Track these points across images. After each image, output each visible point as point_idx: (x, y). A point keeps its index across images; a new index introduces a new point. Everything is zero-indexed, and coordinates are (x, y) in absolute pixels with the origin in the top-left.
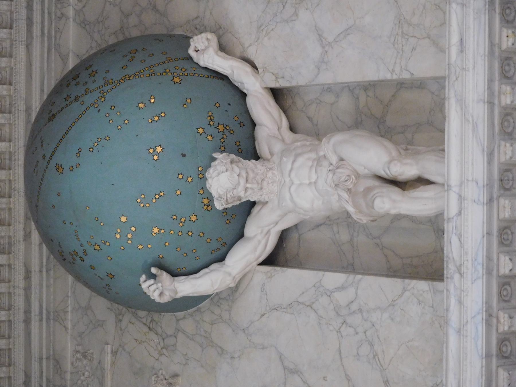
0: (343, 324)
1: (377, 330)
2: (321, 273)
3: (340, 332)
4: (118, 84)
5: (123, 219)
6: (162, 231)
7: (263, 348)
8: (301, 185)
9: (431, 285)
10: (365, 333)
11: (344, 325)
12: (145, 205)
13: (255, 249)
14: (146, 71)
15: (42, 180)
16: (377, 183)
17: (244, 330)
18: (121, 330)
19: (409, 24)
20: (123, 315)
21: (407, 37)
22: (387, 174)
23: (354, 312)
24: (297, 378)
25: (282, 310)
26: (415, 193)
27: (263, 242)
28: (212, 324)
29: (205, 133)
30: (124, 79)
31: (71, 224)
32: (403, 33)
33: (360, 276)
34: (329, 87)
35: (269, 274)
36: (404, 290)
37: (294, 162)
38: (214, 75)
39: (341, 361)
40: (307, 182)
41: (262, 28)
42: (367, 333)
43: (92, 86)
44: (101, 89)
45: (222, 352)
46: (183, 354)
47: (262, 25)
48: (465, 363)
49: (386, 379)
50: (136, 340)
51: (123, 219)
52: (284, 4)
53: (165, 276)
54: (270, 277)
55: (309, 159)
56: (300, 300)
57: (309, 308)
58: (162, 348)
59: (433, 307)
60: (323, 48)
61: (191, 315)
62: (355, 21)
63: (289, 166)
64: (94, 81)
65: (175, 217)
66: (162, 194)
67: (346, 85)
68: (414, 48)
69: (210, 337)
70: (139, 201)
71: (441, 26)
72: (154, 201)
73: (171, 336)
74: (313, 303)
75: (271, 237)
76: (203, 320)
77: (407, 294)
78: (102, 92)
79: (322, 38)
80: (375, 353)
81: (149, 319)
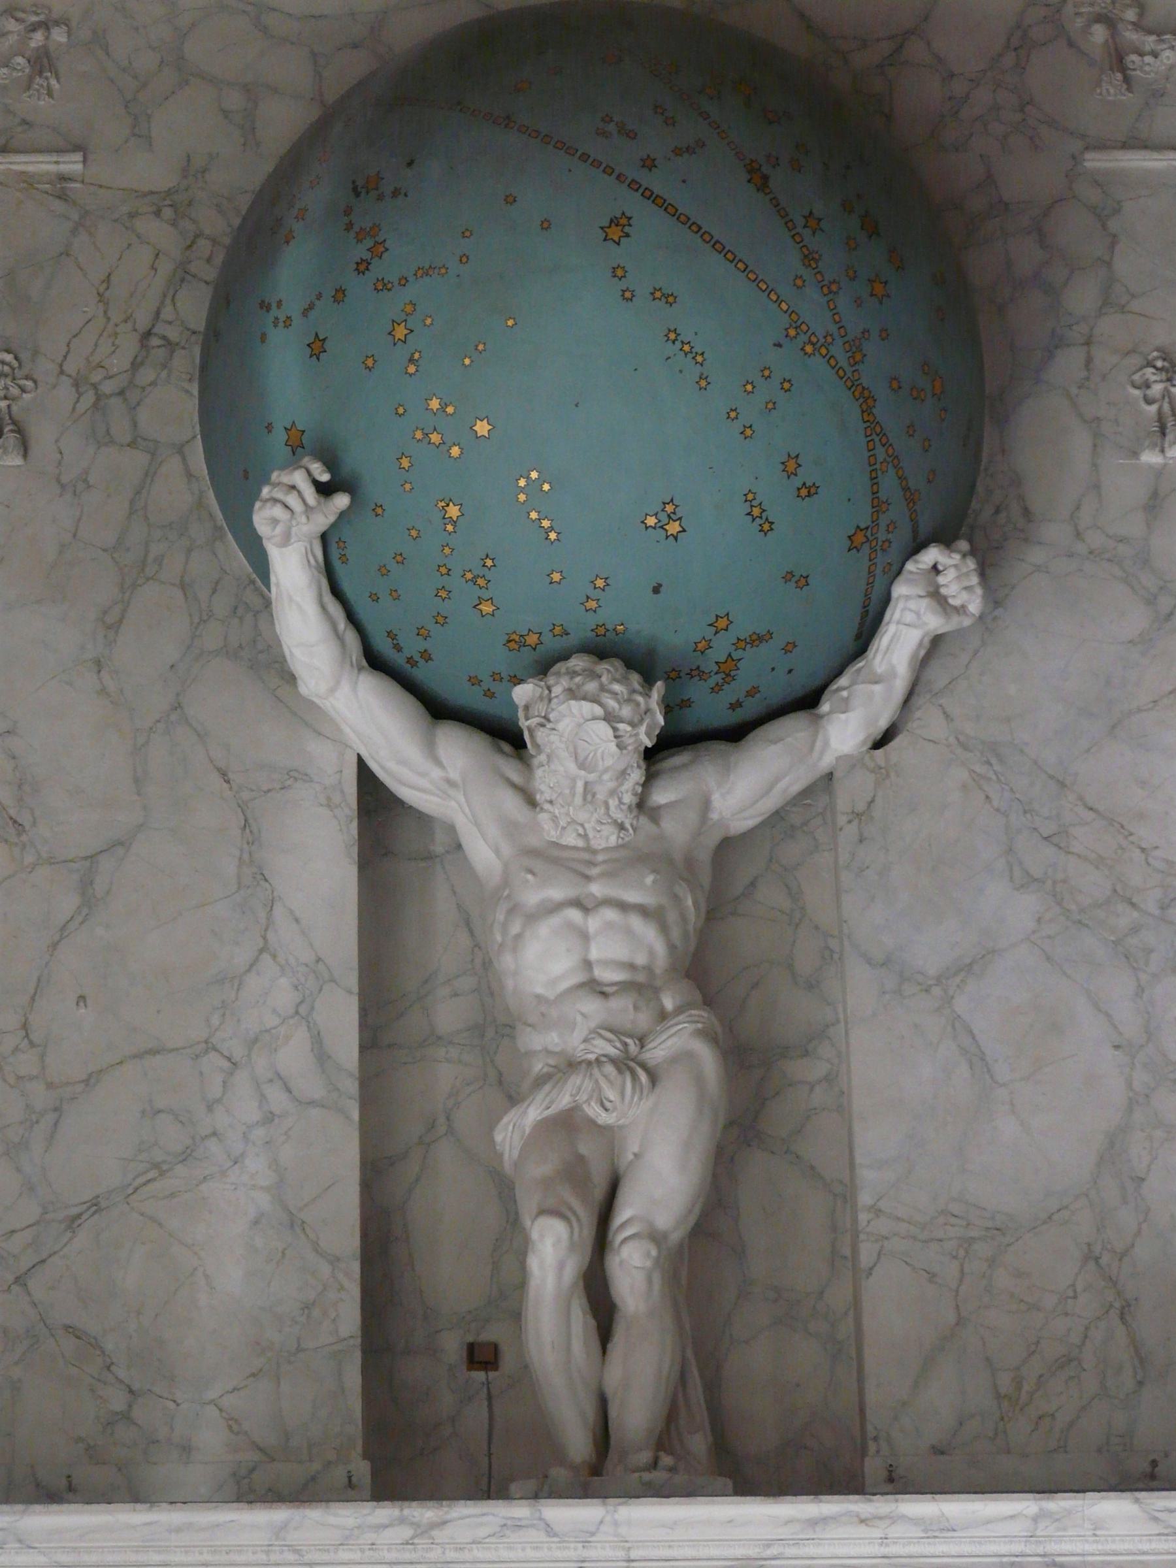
0: (229, 1059)
1: (223, 1173)
2: (353, 981)
3: (206, 1052)
4: (849, 384)
5: (482, 428)
6: (450, 528)
7: (136, 780)
8: (585, 937)
9: (352, 1342)
10: (214, 1134)
11: (226, 1064)
12: (522, 490)
13: (403, 762)
14: (883, 450)
15: (584, 157)
16: (599, 1192)
17: (177, 707)
18: (132, 215)
19: (992, 1262)
20: (174, 224)
21: (962, 1253)
22: (623, 1225)
23: (263, 1098)
24: (68, 903)
25: (245, 846)
26: (580, 1314)
27: (422, 782)
28: (183, 586)
29: (716, 633)
30: (866, 400)
31: (464, 259)
32: (971, 1240)
33: (356, 1115)
34: (836, 956)
35: (337, 798)
36: (334, 1261)
37: (643, 911)
38: (872, 609)
39: (135, 1056)
40: (594, 954)
41: (994, 761)
42: (214, 1139)
43: (843, 302)
44: (836, 334)
45: (111, 625)
46: (86, 472)
47: (1001, 761)
48: (205, 1549)
49: (103, 1204)
50: (108, 279)
51: (482, 428)
52: (1055, 840)
53: (323, 520)
54: (329, 805)
55: (652, 953)
56: (278, 910)
57: (261, 945)
58: (95, 386)
59: (299, 1350)
60: (939, 980)
61: (200, 504)
62: (1004, 1085)
63: (632, 896)
64: (858, 302)
65: (489, 563)
66: (553, 536)
67: (841, 1016)
68: (934, 1275)
69: (148, 579)
70: (534, 475)
71: (987, 1359)
72: (534, 515)
73: (135, 425)
74: (274, 957)
75: (432, 798)
76: (189, 551)
77: (325, 1269)
78: (829, 339)
79: (963, 974)
80: (165, 1167)
81: (173, 334)
